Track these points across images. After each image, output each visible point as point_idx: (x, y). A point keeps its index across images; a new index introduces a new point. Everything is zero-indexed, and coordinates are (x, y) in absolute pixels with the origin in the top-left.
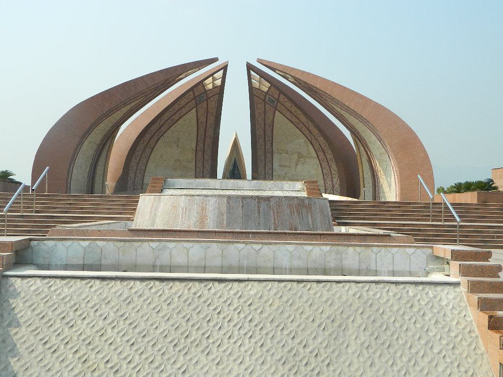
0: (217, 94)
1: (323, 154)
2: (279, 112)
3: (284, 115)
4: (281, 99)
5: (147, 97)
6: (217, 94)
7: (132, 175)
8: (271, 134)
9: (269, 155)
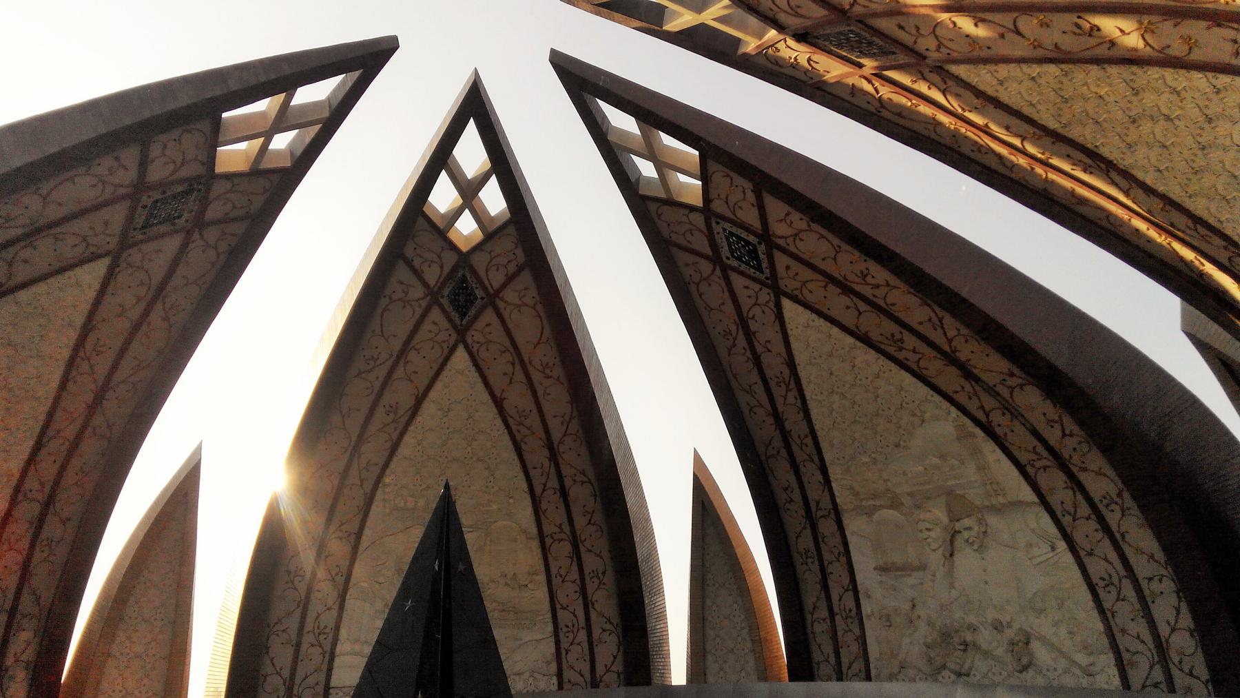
0: (520, 270)
1: (1059, 479)
2: (795, 299)
3: (820, 314)
6: (520, 270)
7: (280, 653)
9: (827, 527)
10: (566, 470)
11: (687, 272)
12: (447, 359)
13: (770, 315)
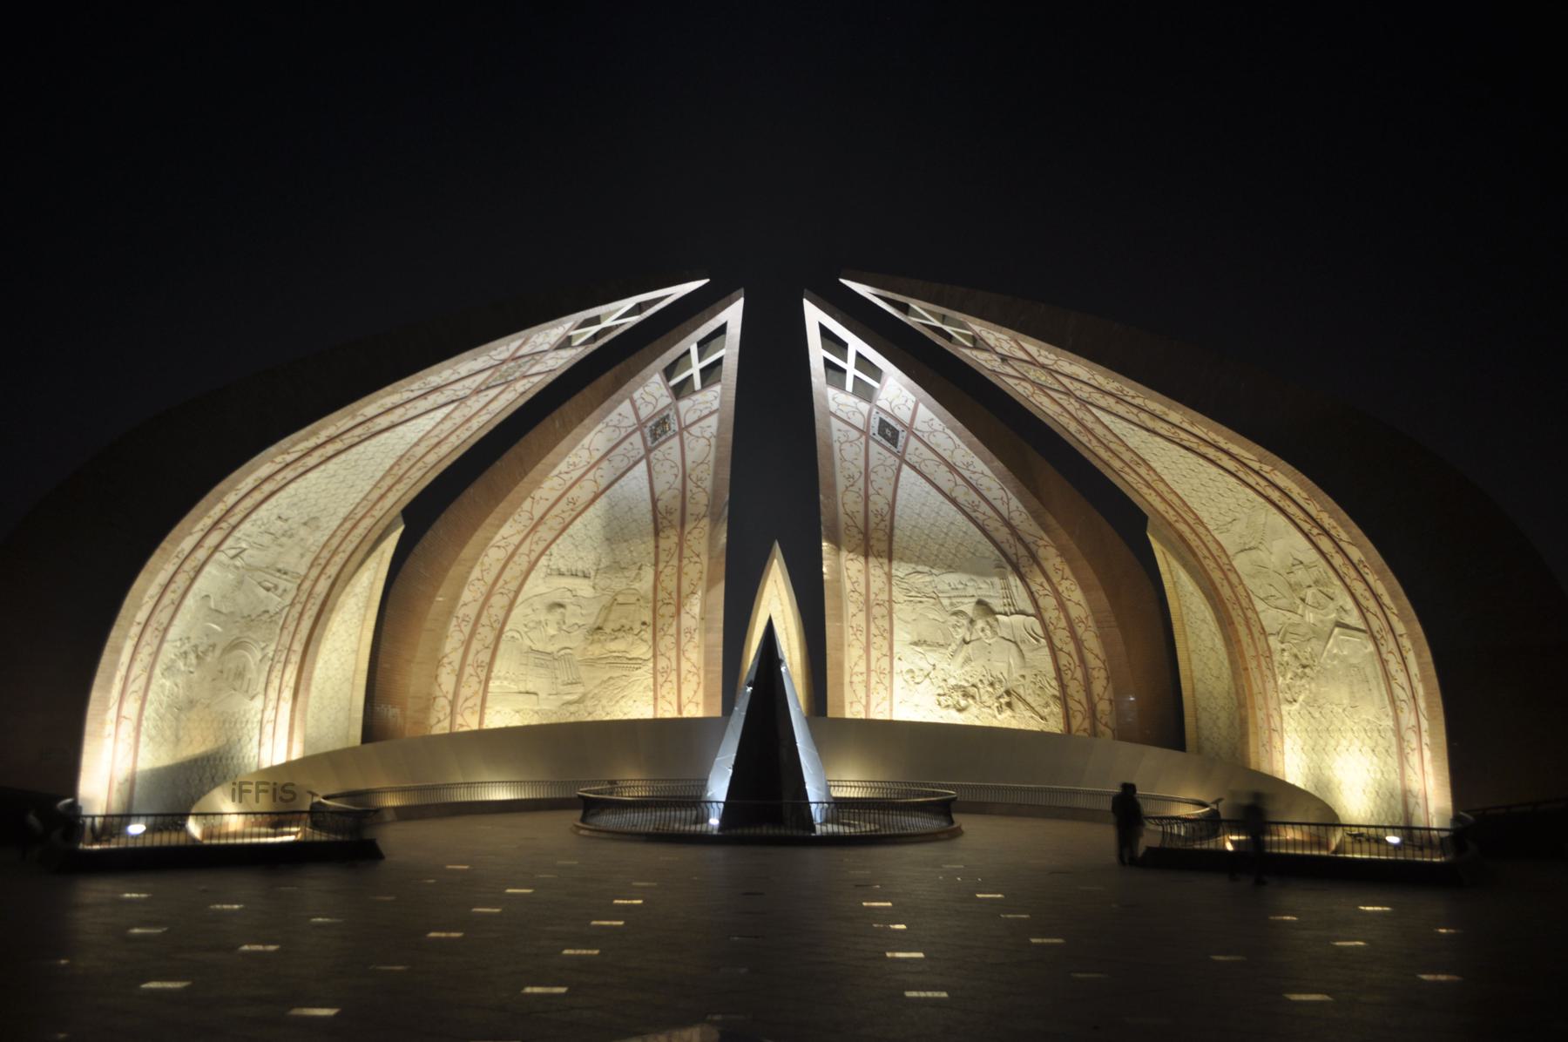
0: (711, 413)
2: (913, 468)
4: (918, 424)
5: (464, 411)
6: (711, 413)
8: (884, 546)
10: (687, 552)
11: (836, 435)
12: (629, 469)
13: (890, 473)
